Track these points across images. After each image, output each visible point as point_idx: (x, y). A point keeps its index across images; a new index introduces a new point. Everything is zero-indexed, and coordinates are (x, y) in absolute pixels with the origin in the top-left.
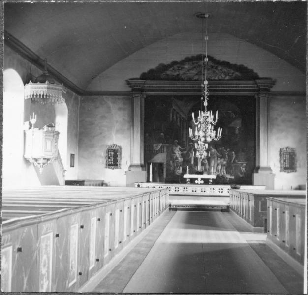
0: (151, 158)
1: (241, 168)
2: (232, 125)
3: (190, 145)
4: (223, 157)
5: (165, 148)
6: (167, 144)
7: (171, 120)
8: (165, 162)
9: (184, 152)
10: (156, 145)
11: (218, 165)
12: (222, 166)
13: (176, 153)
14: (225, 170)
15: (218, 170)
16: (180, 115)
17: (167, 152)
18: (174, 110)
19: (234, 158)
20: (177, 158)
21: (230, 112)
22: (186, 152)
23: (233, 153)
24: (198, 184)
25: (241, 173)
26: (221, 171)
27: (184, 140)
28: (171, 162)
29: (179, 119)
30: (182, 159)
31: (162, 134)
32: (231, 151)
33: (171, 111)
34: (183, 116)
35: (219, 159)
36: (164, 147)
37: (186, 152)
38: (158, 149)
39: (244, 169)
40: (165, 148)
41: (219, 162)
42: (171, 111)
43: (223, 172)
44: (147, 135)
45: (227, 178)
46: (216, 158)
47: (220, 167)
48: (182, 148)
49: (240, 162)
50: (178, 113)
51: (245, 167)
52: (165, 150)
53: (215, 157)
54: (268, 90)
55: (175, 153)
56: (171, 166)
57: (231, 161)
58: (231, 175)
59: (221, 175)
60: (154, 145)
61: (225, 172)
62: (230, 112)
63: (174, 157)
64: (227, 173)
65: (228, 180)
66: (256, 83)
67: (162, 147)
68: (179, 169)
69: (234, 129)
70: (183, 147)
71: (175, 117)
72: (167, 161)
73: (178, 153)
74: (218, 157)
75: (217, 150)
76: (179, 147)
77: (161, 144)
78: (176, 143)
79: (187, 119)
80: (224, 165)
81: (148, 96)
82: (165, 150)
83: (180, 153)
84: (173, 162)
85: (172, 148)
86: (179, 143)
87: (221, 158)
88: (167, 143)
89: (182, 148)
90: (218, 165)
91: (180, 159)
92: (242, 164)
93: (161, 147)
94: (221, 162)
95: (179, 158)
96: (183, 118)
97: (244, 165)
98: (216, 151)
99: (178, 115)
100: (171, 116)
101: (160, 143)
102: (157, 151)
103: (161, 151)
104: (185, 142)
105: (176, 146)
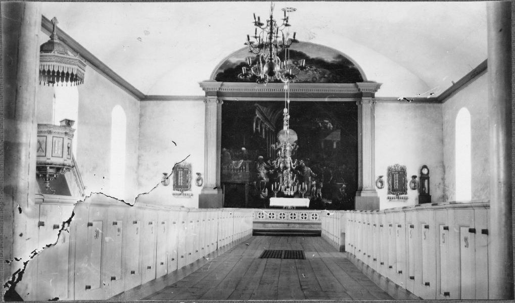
1: (340, 189)
2: (328, 138)
6: (250, 161)
10: (236, 162)
14: (320, 193)
16: (266, 125)
20: (262, 179)
21: (327, 121)
26: (316, 194)
29: (264, 130)
30: (268, 180)
31: (243, 149)
33: (255, 120)
37: (273, 170)
39: (343, 190)
45: (323, 202)
54: (373, 96)
55: (259, 172)
58: (329, 199)
62: (327, 121)
66: (357, 86)
68: (265, 192)
69: (331, 143)
71: (259, 128)
74: (312, 176)
77: (242, 161)
81: (225, 101)
83: (265, 171)
90: (312, 186)
91: (265, 179)
92: (342, 185)
95: (264, 178)
98: (309, 168)
99: (263, 126)
101: (240, 160)
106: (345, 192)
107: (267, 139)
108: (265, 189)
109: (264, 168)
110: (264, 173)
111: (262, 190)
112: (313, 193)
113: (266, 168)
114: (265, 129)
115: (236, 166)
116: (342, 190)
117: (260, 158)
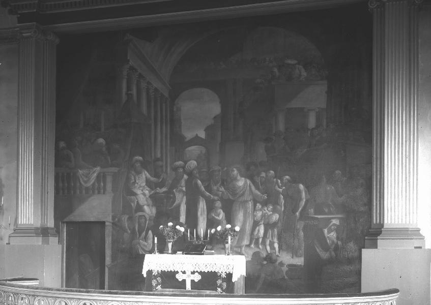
0: (70, 210)
1: (326, 231)
3: (175, 169)
4: (270, 199)
5: (109, 179)
6: (115, 170)
7: (124, 98)
8: (108, 219)
9: (159, 190)
11: (256, 224)
12: (269, 226)
13: (139, 192)
14: (275, 240)
15: (254, 240)
16: (149, 83)
17: (114, 189)
18: (132, 68)
19: (303, 203)
20: (140, 208)
22: (164, 189)
23: (301, 187)
24: (170, 280)
25: (326, 248)
26: (264, 243)
27: (159, 155)
28: (125, 218)
30: (154, 210)
31: (101, 140)
32: (294, 181)
33: (125, 73)
34: (156, 84)
35: (259, 206)
36: (104, 177)
37: (164, 189)
38: (89, 184)
39: (333, 235)
40: (109, 179)
41: (259, 214)
42: (125, 73)
43: (272, 244)
44: (62, 144)
45: (281, 264)
46: (250, 205)
47: (262, 229)
48: (153, 179)
49: (324, 213)
50: (141, 76)
51: (338, 229)
52: (109, 186)
53: (247, 201)
55: (135, 194)
56: (125, 231)
57: (294, 211)
58: (295, 253)
59: (264, 254)
60: (80, 172)
61: (276, 245)
63: (134, 205)
64: (280, 248)
65: (285, 269)
67: (101, 178)
68: (146, 239)
70: (156, 175)
72: (113, 218)
73: (142, 194)
75: (251, 178)
76: (145, 175)
77: (98, 169)
78: (138, 165)
79: (166, 94)
80: (274, 225)
82: (109, 186)
84: (131, 219)
85: (128, 179)
86: (145, 165)
87: (265, 204)
88: (112, 166)
89: (153, 179)
90: (256, 224)
91: (149, 211)
92: (329, 220)
93: (98, 177)
94: (263, 216)
95: (146, 208)
96: (156, 89)
97: (335, 222)
98: (248, 182)
99: (143, 85)
100: (124, 90)
101: (95, 167)
102: (87, 189)
103: (99, 189)
104: (161, 159)
105: (139, 173)
106: (338, 238)
107: (153, 115)
108: (147, 233)
109: (144, 184)
110: (144, 194)
111: (140, 235)
112: (257, 240)
113: (148, 183)
114: (148, 93)
115: (86, 182)
116: (329, 233)
117: (137, 161)
